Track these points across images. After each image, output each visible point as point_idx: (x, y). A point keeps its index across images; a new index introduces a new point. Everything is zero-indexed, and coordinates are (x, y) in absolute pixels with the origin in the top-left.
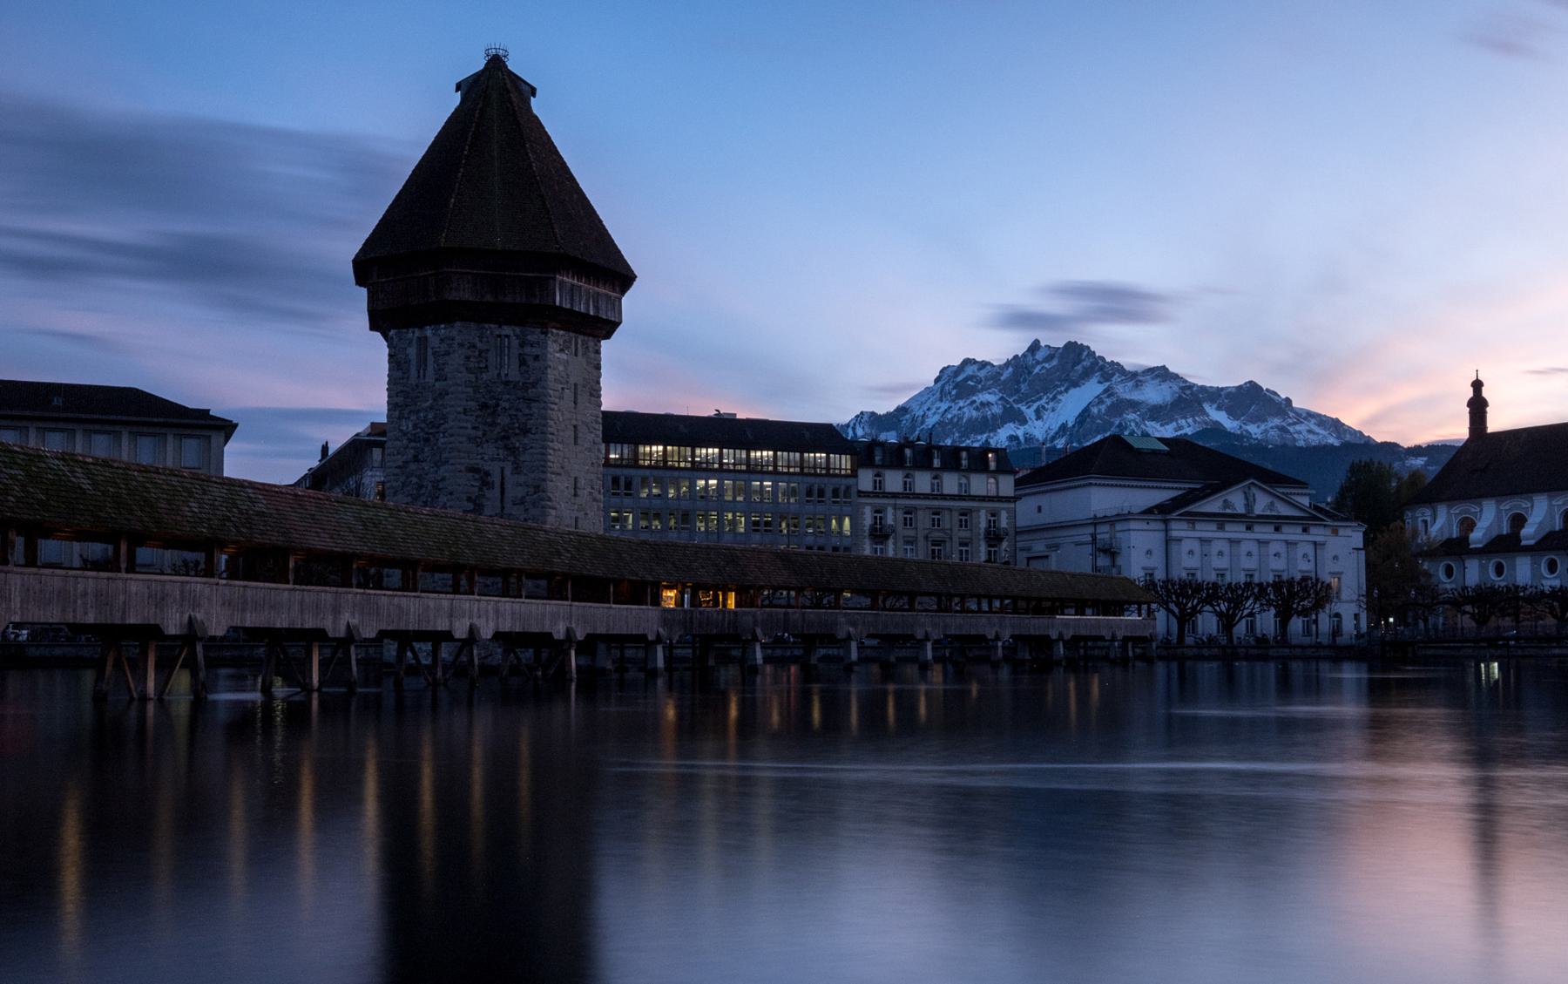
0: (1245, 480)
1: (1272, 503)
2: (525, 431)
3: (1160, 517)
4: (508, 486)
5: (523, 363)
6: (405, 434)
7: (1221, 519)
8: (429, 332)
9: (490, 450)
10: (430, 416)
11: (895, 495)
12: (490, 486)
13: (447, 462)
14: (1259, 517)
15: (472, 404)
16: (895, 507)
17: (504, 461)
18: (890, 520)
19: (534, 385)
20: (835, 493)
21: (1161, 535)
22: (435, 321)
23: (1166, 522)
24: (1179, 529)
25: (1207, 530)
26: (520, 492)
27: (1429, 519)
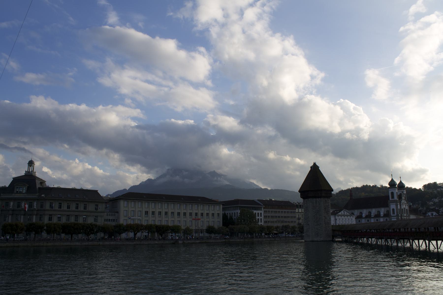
0: (343, 210)
1: (346, 213)
4: (328, 219)
5: (328, 203)
6: (314, 212)
7: (341, 215)
8: (317, 199)
11: (301, 213)
12: (325, 218)
14: (346, 215)
16: (300, 215)
18: (300, 217)
20: (284, 212)
21: (334, 218)
23: (335, 216)
24: (337, 217)
25: (340, 217)
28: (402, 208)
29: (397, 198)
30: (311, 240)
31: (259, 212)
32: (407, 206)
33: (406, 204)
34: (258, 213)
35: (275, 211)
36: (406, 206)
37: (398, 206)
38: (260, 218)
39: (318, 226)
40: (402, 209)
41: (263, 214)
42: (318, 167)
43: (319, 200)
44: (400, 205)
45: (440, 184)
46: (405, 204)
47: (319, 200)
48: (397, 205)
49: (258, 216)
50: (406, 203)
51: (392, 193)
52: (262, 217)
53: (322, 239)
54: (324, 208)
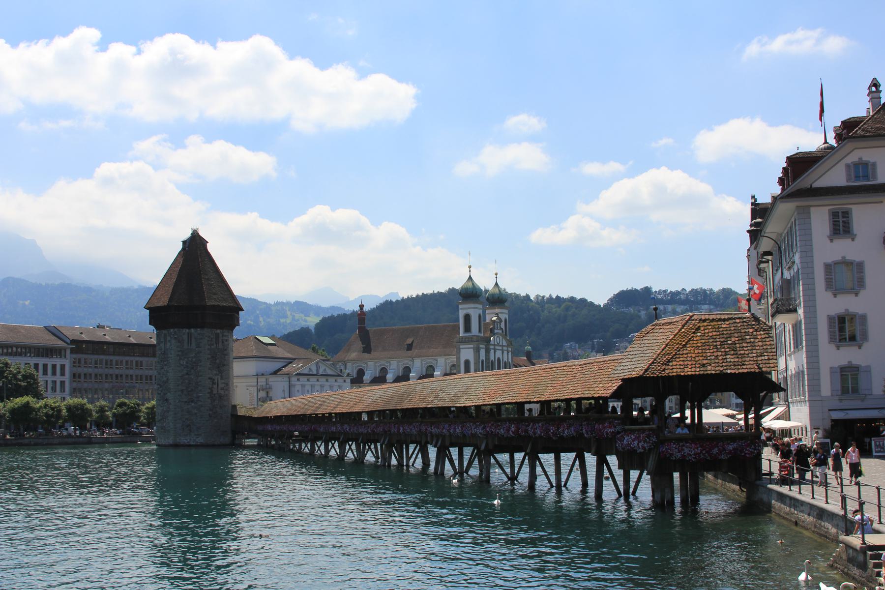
1: (325, 369)
2: (224, 365)
3: (288, 376)
5: (223, 342)
8: (193, 330)
9: (215, 372)
10: (194, 360)
12: (214, 383)
13: (201, 376)
14: (322, 375)
15: (210, 356)
17: (218, 375)
19: (226, 350)
22: (195, 327)
23: (289, 378)
25: (303, 379)
26: (223, 385)
27: (342, 368)
28: (492, 358)
29: (480, 331)
30: (171, 442)
31: (58, 362)
32: (508, 354)
33: (505, 348)
34: (54, 366)
35: (106, 361)
36: (505, 352)
37: (479, 352)
38: (58, 378)
39: (193, 404)
40: (492, 361)
41: (70, 367)
42: (203, 243)
43: (199, 334)
44: (488, 351)
45: (660, 292)
46: (500, 348)
47: (199, 334)
48: (477, 351)
49: (54, 373)
50: (505, 343)
51: (467, 318)
52: (67, 378)
53: (200, 440)
54: (210, 356)
